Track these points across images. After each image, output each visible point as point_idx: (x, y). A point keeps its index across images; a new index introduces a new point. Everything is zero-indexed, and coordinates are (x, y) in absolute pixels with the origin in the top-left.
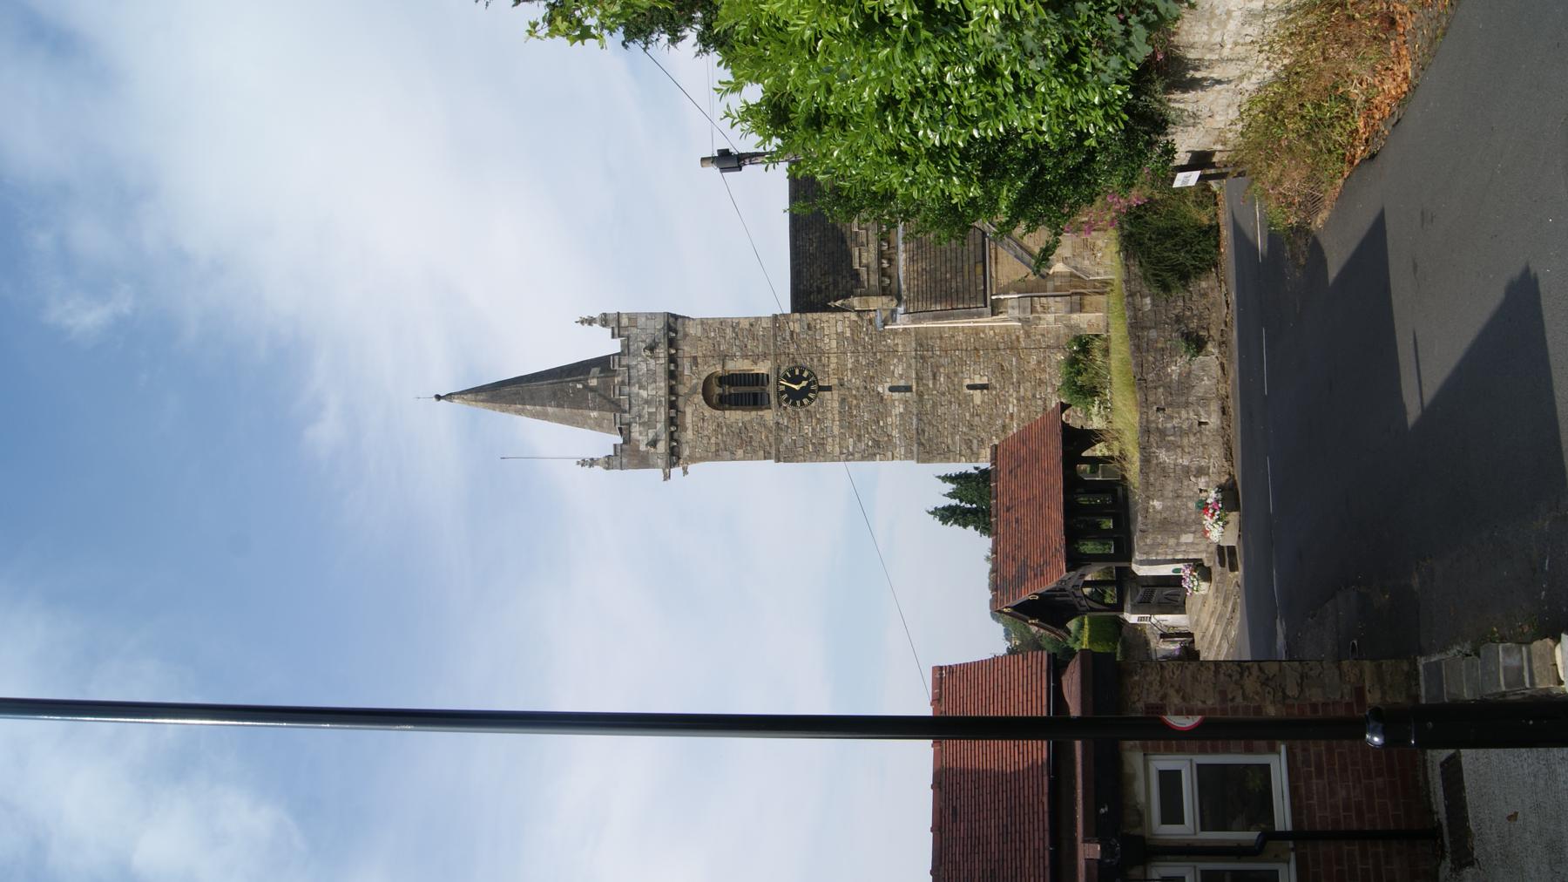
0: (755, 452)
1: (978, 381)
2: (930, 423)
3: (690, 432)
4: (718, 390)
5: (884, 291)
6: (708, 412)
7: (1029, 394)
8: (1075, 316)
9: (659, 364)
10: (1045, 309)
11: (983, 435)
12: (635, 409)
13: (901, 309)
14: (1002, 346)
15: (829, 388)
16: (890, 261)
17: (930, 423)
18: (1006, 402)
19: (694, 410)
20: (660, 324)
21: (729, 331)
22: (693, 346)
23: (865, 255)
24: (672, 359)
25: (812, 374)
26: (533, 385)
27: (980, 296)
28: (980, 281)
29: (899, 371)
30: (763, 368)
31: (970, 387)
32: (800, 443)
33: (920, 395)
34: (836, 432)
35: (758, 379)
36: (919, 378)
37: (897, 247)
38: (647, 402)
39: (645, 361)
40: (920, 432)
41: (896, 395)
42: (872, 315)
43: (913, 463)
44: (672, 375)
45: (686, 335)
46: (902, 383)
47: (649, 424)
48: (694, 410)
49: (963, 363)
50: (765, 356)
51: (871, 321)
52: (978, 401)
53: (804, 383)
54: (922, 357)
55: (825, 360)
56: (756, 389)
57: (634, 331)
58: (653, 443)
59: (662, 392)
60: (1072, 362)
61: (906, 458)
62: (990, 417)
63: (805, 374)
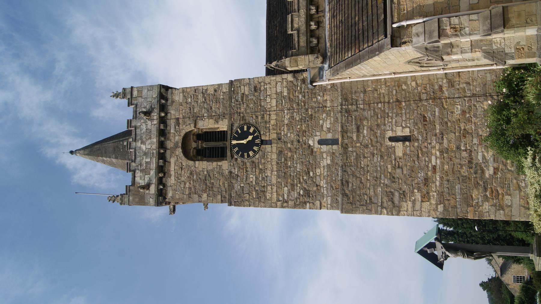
0: (215, 196)
1: (400, 132)
2: (354, 175)
3: (173, 178)
4: (194, 145)
5: (312, 50)
6: (185, 162)
7: (453, 146)
8: (497, 37)
10: (458, 31)
11: (405, 187)
12: (138, 159)
13: (326, 66)
14: (424, 97)
15: (269, 142)
16: (319, 24)
17: (354, 175)
18: (428, 154)
19: (176, 160)
20: (155, 94)
22: (178, 110)
23: (296, 19)
24: (163, 121)
25: (257, 130)
26: (106, 144)
27: (381, 29)
28: (381, 11)
29: (327, 125)
30: (223, 126)
31: (392, 139)
32: (246, 190)
33: (345, 148)
34: (274, 181)
35: (221, 136)
36: (344, 132)
37: (324, 11)
38: (145, 154)
39: (145, 122)
40: (344, 183)
41: (324, 148)
42: (305, 75)
43: (338, 212)
44: (162, 133)
45: (173, 102)
46: (329, 136)
47: (145, 171)
48: (176, 160)
49: (385, 115)
50: (224, 116)
51: (304, 81)
53: (250, 138)
54: (348, 111)
55: (267, 117)
56: (220, 144)
57: (140, 100)
59: (154, 146)
60: (500, 108)
61: (332, 208)
62: (412, 170)
63: (251, 130)
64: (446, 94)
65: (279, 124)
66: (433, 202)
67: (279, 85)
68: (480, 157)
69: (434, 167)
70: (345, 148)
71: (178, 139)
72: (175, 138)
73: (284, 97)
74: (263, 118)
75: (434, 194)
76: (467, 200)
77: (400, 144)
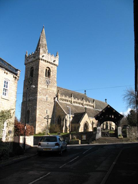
1: (48, 112)
9: (52, 62)
34: (42, 87)
36: (48, 102)
41: (46, 98)
46: (48, 99)
52: (45, 111)
55: (51, 88)
72: (50, 66)
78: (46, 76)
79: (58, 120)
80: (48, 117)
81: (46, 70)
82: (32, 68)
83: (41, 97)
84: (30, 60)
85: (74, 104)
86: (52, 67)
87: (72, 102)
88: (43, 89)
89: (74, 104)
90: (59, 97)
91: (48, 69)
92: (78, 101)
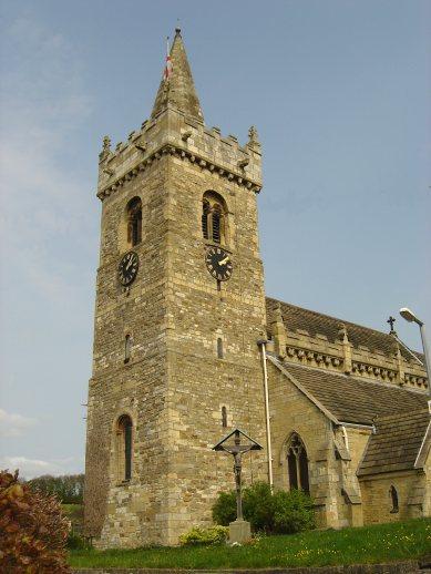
1: (229, 416)
4: (212, 203)
9: (232, 166)
15: (219, 290)
21: (250, 226)
23: (306, 339)
31: (224, 408)
34: (190, 285)
36: (229, 365)
46: (224, 350)
58: (185, 140)
64: (254, 462)
65: (232, 303)
66: (178, 442)
67: (260, 311)
68: (213, 487)
69: (205, 446)
70: (217, 364)
71: (220, 190)
72: (223, 187)
73: (250, 313)
74: (237, 287)
75: (184, 443)
76: (182, 474)
77: (221, 417)
78: (206, 237)
79: (291, 458)
80: (237, 442)
81: (206, 206)
82: (136, 200)
83: (189, 336)
84: (121, 171)
85: (357, 376)
86: (233, 194)
87: (348, 362)
88: (197, 297)
89: (357, 376)
90: (283, 340)
91: (212, 203)
92: (372, 361)
